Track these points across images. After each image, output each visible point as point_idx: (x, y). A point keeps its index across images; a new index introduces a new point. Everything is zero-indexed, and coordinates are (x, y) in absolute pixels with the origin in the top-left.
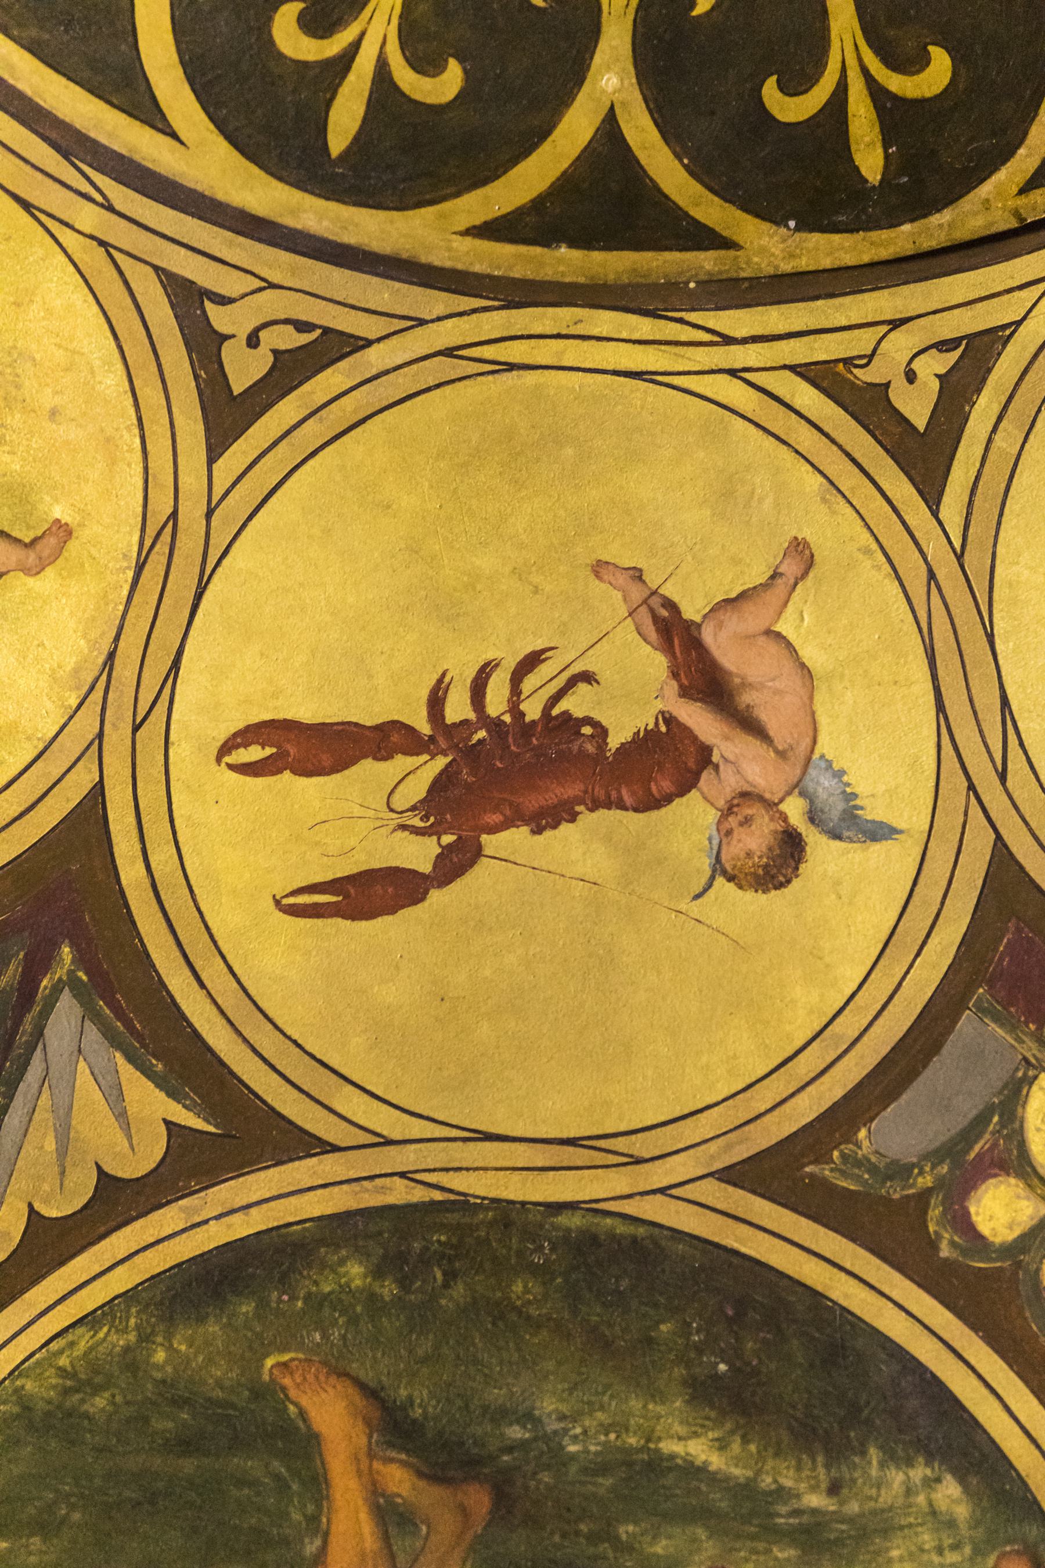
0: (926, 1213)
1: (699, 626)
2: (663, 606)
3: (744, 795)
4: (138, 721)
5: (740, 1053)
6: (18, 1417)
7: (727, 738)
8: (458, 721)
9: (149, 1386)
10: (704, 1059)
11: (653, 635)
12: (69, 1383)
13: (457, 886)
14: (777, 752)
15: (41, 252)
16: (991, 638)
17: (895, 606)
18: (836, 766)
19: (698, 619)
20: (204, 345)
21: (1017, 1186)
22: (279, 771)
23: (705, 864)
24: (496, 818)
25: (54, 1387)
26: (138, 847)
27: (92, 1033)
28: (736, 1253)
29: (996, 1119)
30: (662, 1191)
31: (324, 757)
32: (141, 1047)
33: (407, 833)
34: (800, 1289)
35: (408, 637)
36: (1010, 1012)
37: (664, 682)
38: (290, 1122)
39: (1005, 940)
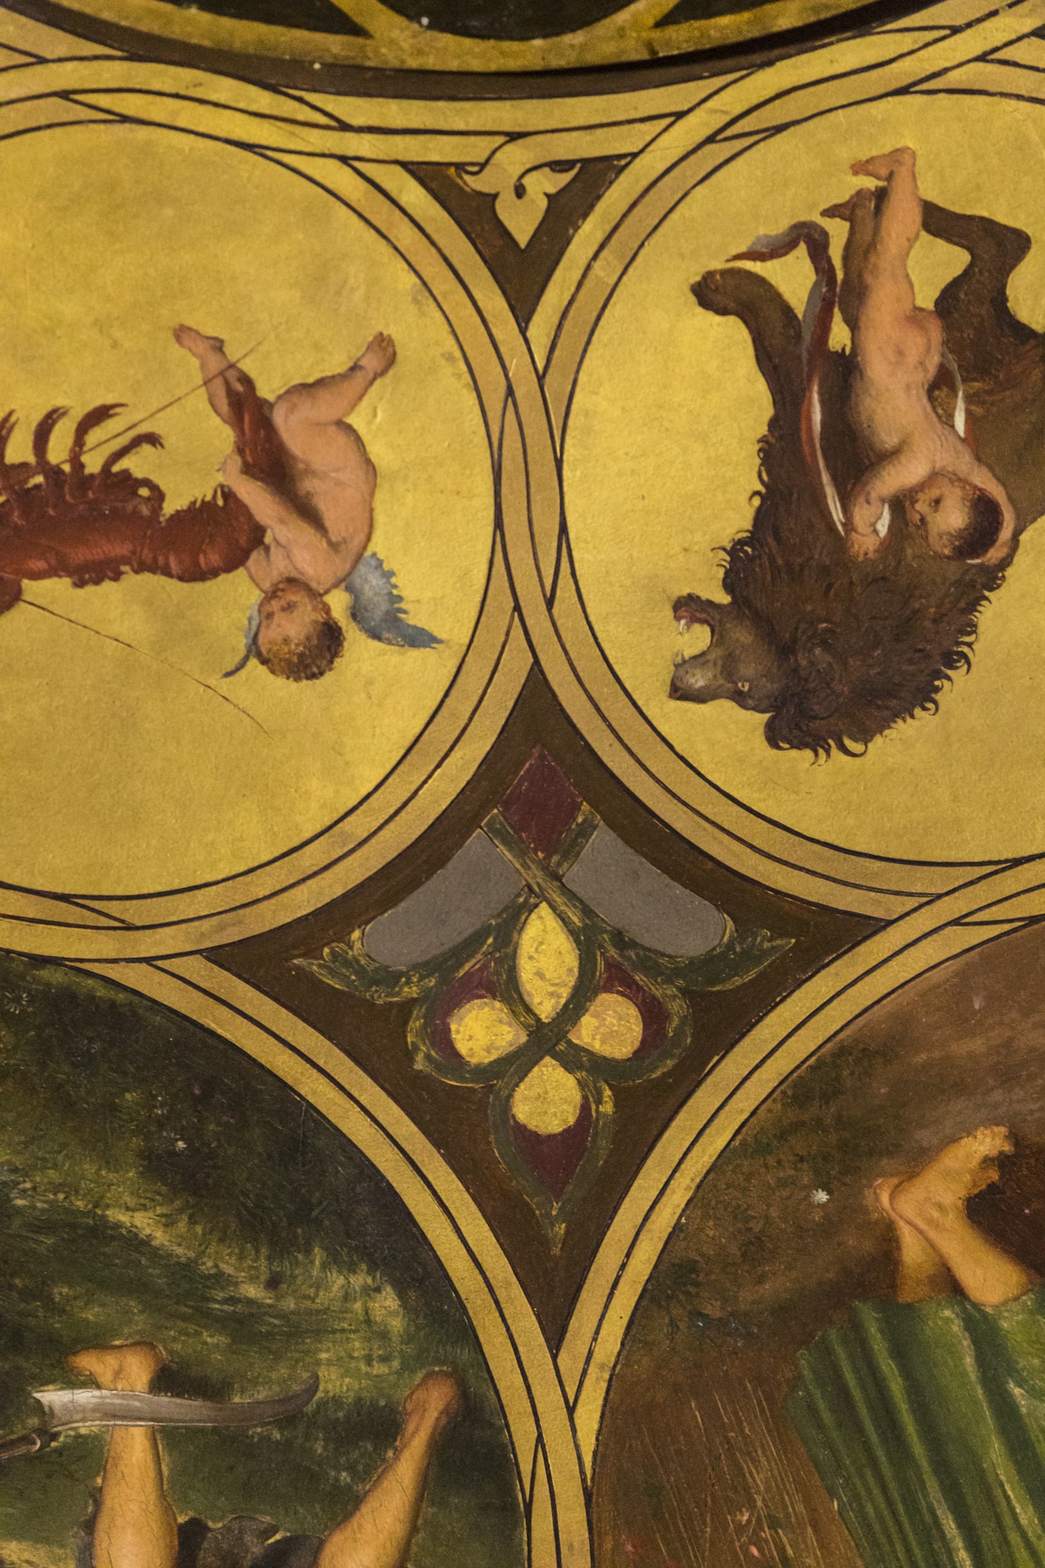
0: (406, 1023)
1: (271, 406)
2: (239, 380)
3: (291, 581)
5: (245, 836)
7: (282, 521)
10: (210, 837)
11: (225, 408)
14: (330, 543)
16: (559, 463)
17: (470, 417)
18: (386, 566)
19: (271, 397)
21: (502, 1010)
23: (241, 644)
24: (40, 565)
28: (212, 1033)
29: (490, 941)
30: (148, 960)
34: (270, 1079)
36: (521, 837)
37: (229, 456)
39: (527, 765)
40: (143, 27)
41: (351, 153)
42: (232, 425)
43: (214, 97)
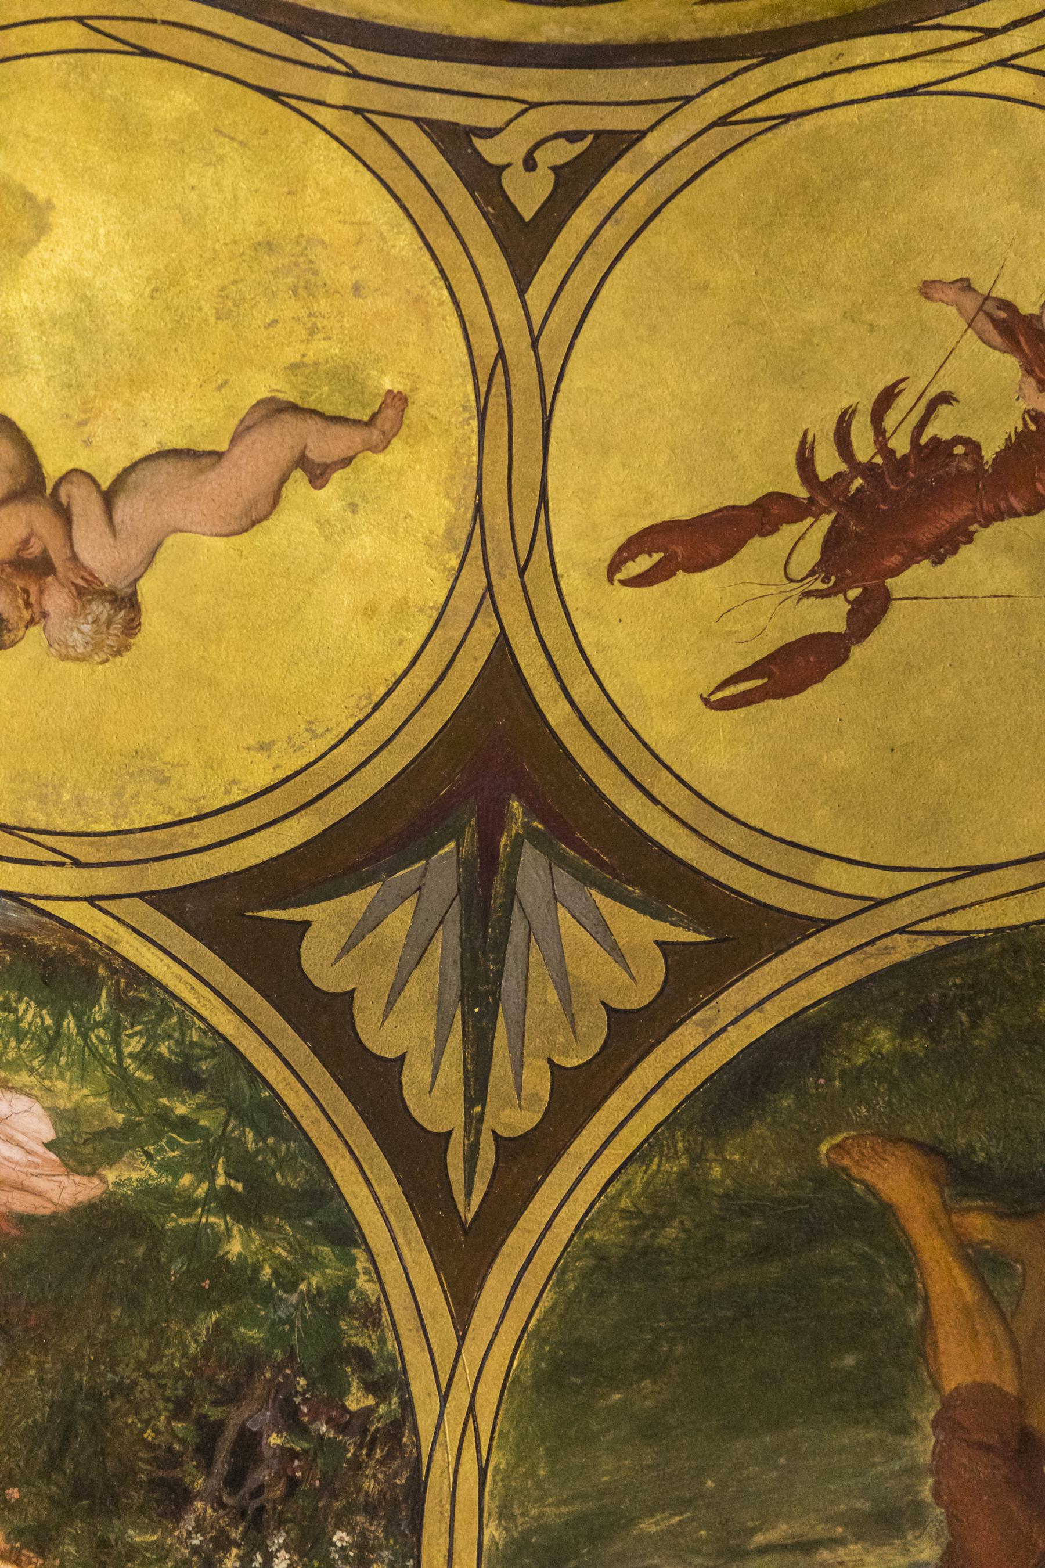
2: (999, 308)
4: (522, 563)
6: (595, 1269)
8: (831, 476)
9: (714, 1203)
11: (998, 340)
12: (635, 1223)
13: (876, 637)
15: (301, 137)
20: (484, 181)
22: (673, 574)
24: (896, 559)
25: (621, 1231)
26: (556, 685)
27: (564, 879)
31: (710, 547)
32: (615, 878)
33: (813, 599)
35: (760, 409)
37: (1022, 381)
38: (779, 910)
40: (766, 26)
41: (1006, 54)
42: (1011, 352)
43: (858, 61)
